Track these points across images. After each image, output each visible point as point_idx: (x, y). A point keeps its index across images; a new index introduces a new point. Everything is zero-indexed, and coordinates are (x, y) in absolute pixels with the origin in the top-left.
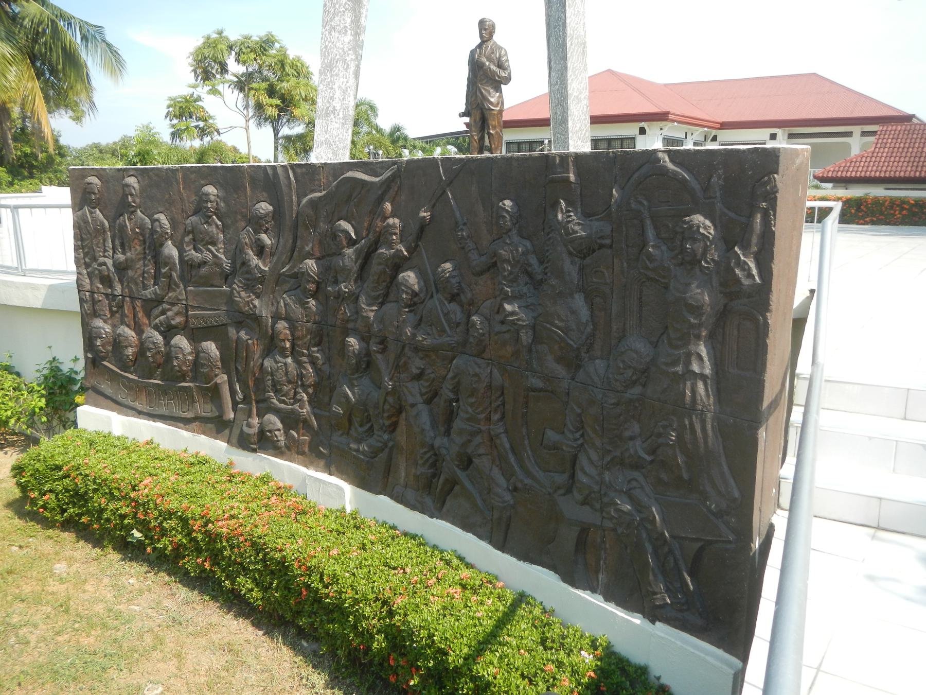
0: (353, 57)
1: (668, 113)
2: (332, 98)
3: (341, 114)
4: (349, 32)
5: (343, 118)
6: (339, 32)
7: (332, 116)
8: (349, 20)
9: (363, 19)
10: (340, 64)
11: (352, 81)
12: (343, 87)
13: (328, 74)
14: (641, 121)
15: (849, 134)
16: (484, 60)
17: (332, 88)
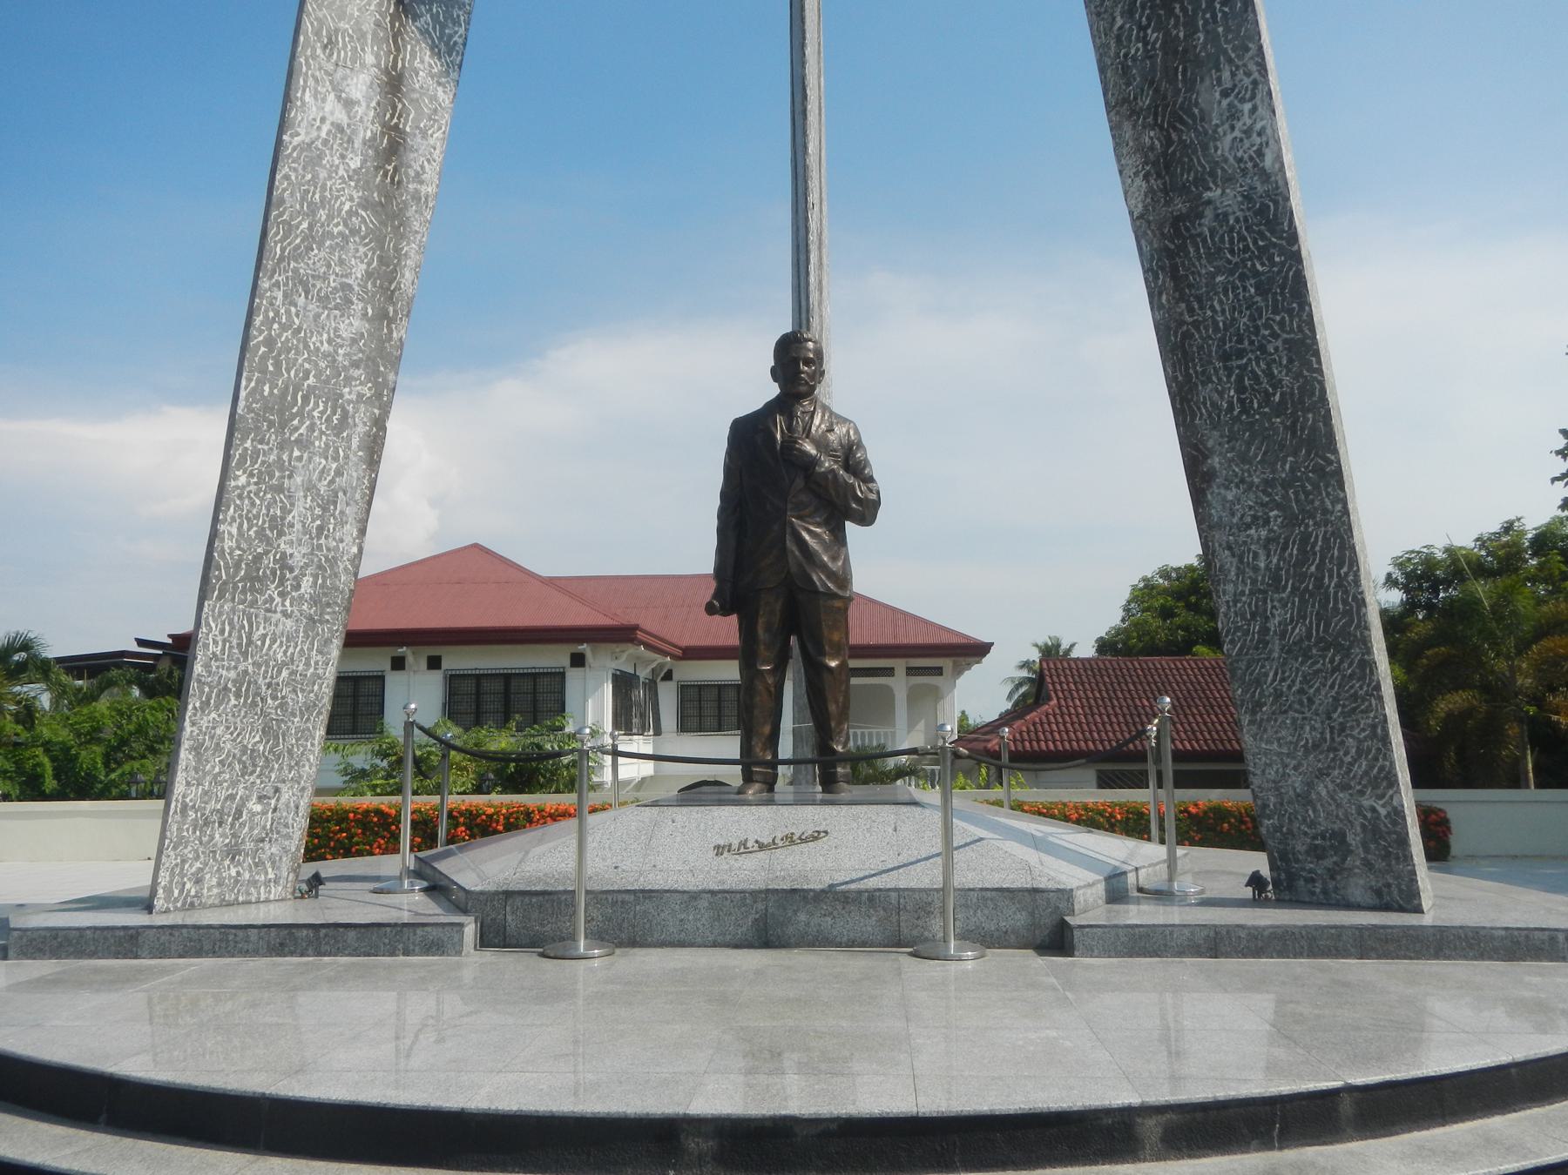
0: (366, 391)
1: (636, 628)
2: (278, 526)
3: (306, 583)
4: (358, 306)
5: (315, 601)
6: (324, 300)
7: (273, 590)
8: (360, 270)
9: (407, 274)
10: (317, 409)
11: (355, 473)
12: (323, 487)
13: (273, 438)
14: (581, 641)
15: (889, 672)
16: (809, 448)
17: (279, 489)
